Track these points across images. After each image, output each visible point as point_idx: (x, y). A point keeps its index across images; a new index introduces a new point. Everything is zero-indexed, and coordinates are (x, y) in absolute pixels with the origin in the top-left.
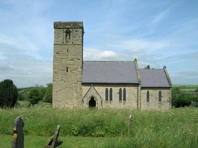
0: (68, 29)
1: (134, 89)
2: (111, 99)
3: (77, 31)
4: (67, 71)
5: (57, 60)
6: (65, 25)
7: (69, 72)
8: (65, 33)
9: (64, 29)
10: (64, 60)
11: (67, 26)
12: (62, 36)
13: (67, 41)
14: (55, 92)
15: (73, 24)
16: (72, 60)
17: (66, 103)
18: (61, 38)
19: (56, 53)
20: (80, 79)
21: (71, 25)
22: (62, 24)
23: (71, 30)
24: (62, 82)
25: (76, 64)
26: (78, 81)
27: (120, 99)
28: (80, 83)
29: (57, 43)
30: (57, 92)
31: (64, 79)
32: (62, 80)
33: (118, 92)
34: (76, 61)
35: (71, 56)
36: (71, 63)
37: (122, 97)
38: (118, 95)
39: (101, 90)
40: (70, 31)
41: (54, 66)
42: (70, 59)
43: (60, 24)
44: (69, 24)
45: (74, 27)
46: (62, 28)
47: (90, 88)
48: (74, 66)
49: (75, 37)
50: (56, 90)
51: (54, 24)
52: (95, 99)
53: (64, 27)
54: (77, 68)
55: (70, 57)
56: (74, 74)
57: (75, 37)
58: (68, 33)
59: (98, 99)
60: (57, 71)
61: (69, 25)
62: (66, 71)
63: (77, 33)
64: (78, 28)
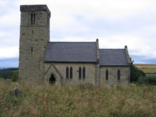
0: (33, 11)
1: (92, 67)
2: (71, 77)
3: (41, 14)
4: (32, 51)
5: (23, 40)
6: (31, 8)
7: (34, 51)
8: (30, 16)
9: (29, 12)
10: (29, 41)
11: (32, 9)
12: (27, 18)
13: (31, 23)
14: (21, 70)
15: (37, 7)
16: (36, 40)
17: (31, 80)
18: (26, 20)
19: (21, 34)
20: (43, 58)
21: (36, 8)
22: (27, 7)
23: (36, 12)
24: (27, 61)
25: (40, 45)
26: (41, 60)
27: (80, 77)
28: (43, 61)
29: (23, 25)
30: (23, 70)
31: (29, 58)
32: (27, 59)
33: (78, 70)
34: (40, 42)
35: (35, 37)
36: (36, 44)
37: (82, 73)
38: (78, 73)
39: (62, 68)
40: (35, 13)
41: (20, 46)
42: (35, 40)
43: (26, 7)
44: (34, 7)
45: (38, 10)
46: (27, 11)
47: (50, 65)
48: (38, 46)
49: (39, 19)
50: (22, 69)
51: (20, 7)
52: (54, 77)
53: (29, 10)
54: (41, 48)
55: (35, 38)
56: (38, 53)
57: (39, 19)
58: (33, 16)
59: (57, 76)
60: (23, 51)
61: (34, 8)
62: (31, 51)
63: (41, 15)
64: (42, 11)
